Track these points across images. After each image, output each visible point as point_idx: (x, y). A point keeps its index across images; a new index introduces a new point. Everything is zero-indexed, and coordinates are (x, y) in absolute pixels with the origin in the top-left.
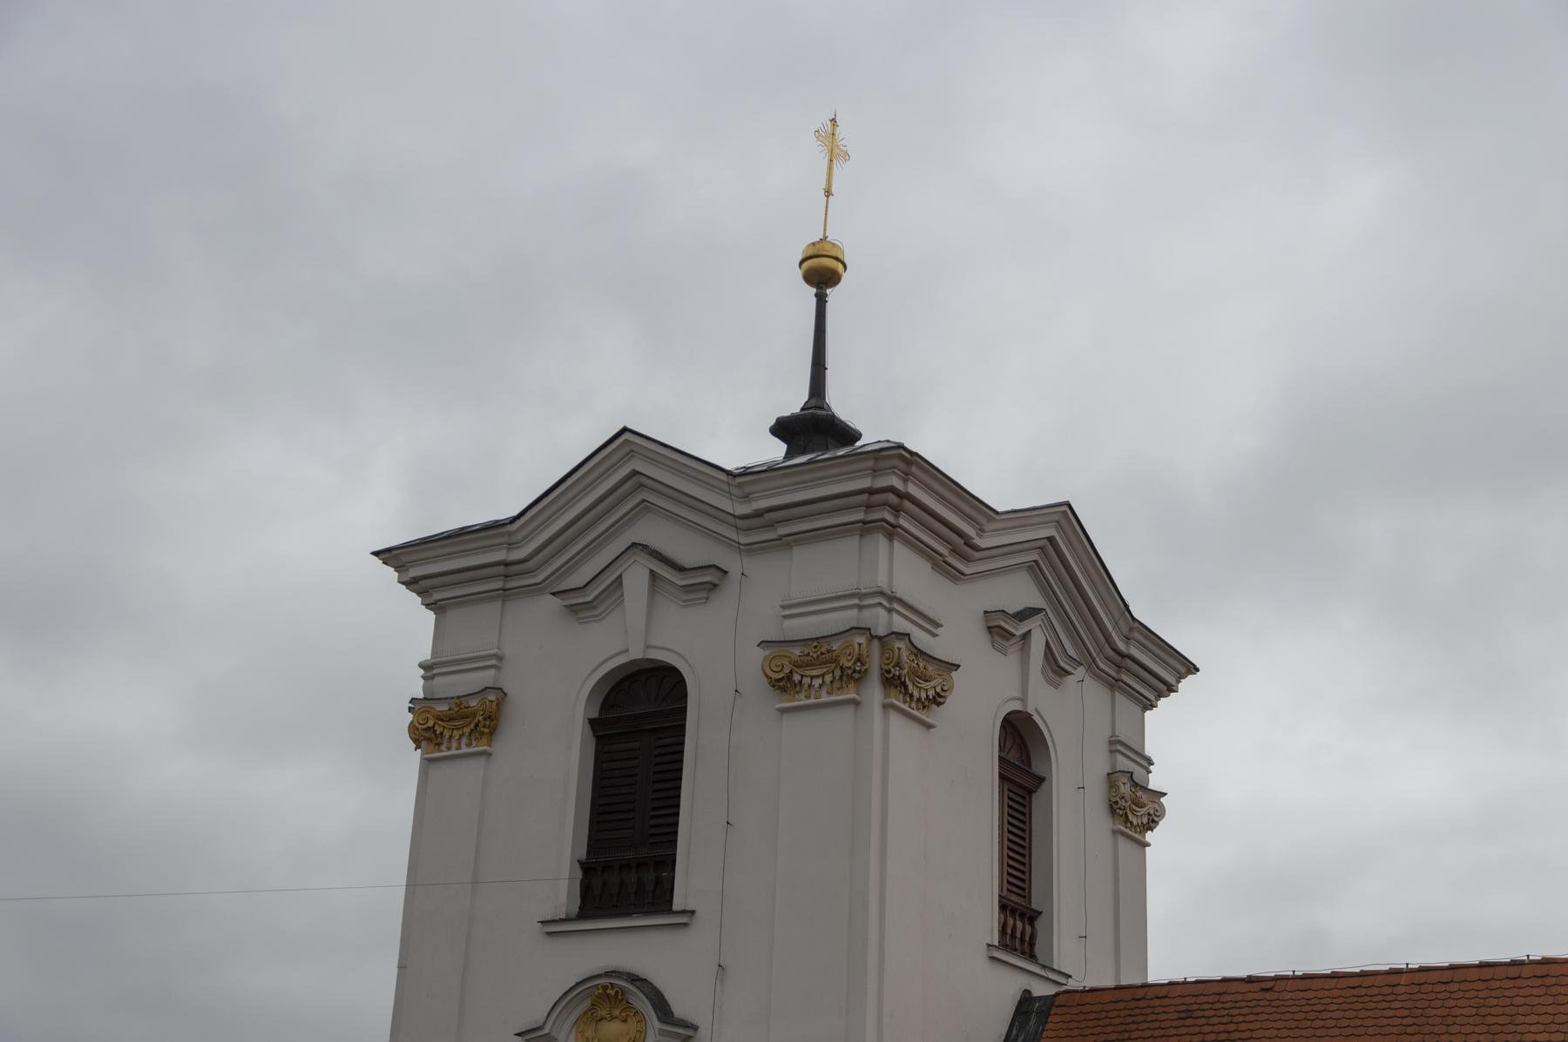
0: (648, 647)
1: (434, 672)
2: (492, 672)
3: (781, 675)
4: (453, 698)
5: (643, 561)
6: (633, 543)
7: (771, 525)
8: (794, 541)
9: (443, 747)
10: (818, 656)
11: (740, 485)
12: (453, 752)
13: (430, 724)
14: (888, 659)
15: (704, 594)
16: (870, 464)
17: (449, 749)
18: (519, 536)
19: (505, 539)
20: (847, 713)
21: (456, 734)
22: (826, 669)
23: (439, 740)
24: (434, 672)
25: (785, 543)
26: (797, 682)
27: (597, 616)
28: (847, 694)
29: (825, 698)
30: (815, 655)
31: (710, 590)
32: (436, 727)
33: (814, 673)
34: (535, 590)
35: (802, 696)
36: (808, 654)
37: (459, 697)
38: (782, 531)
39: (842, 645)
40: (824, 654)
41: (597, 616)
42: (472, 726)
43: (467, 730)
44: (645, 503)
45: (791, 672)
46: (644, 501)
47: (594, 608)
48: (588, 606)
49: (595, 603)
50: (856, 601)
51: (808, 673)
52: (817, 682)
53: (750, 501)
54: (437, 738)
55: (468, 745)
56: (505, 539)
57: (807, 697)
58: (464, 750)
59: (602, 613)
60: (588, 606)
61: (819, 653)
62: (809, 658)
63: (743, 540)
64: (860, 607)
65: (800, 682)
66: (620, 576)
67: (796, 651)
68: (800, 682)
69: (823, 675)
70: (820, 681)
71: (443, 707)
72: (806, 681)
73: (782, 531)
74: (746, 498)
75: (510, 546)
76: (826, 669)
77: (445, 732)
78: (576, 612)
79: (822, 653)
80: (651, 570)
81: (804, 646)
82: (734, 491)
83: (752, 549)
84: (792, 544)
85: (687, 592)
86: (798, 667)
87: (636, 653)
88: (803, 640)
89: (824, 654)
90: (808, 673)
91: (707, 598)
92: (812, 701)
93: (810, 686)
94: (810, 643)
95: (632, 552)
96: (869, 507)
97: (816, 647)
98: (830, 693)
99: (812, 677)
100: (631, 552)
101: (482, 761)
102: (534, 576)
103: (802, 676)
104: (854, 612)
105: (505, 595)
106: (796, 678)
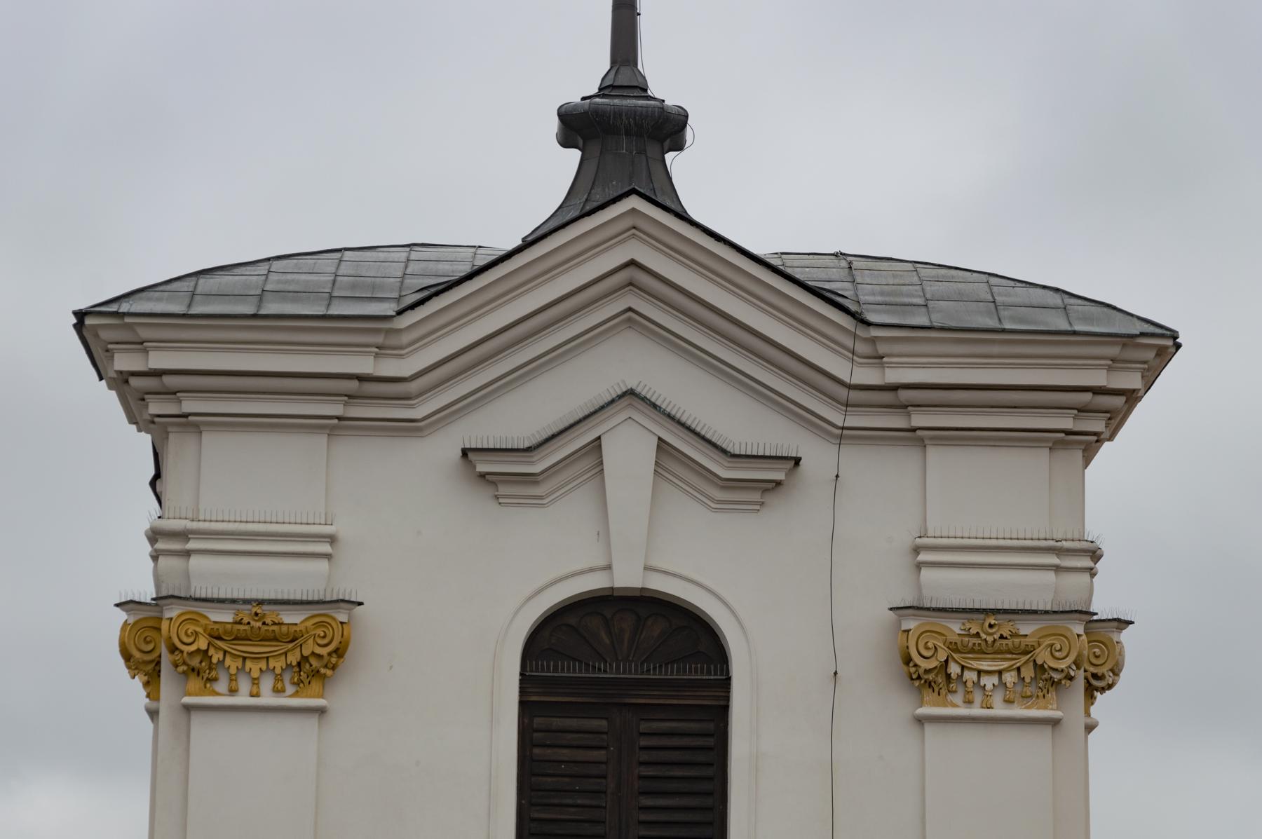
0: (648, 568)
1: (192, 545)
2: (323, 565)
3: (932, 664)
4: (247, 602)
5: (637, 416)
6: (631, 393)
7: (904, 407)
8: (932, 438)
9: (222, 686)
10: (995, 640)
11: (873, 341)
12: (242, 699)
13: (202, 644)
14: (1097, 657)
15: (756, 496)
16: (1114, 351)
17: (233, 691)
18: (405, 338)
19: (379, 339)
20: (1040, 740)
21: (254, 667)
22: (1006, 664)
23: (213, 674)
24: (192, 545)
25: (915, 438)
26: (954, 676)
27: (541, 497)
28: (1046, 708)
29: (1000, 710)
30: (990, 639)
31: (765, 491)
32: (211, 652)
33: (985, 665)
34: (411, 428)
35: (958, 698)
36: (978, 635)
37: (261, 602)
38: (919, 420)
39: (1041, 629)
40: (1006, 638)
41: (541, 497)
42: (293, 658)
43: (278, 664)
44: (630, 314)
45: (946, 661)
46: (630, 309)
47: (536, 483)
48: (529, 479)
49: (540, 478)
50: (1053, 560)
51: (976, 664)
52: (988, 681)
53: (882, 366)
54: (211, 669)
55: (278, 691)
56: (379, 339)
57: (969, 702)
58: (267, 699)
59: (548, 495)
60: (529, 479)
61: (996, 636)
62: (977, 641)
63: (836, 417)
64: (1058, 569)
65: (960, 676)
66: (599, 438)
67: (955, 627)
68: (960, 676)
69: (1000, 673)
70: (995, 680)
71: (224, 616)
72: (970, 676)
73: (919, 420)
74: (878, 359)
75: (382, 351)
76: (1006, 664)
77: (228, 661)
78: (494, 484)
79: (1002, 637)
80: (660, 439)
81: (970, 620)
82: (861, 348)
83: (844, 436)
84: (927, 442)
85: (723, 488)
86: (957, 651)
87: (628, 577)
88: (964, 611)
89: (1006, 638)
90: (976, 664)
91: (762, 504)
92: (976, 711)
93: (977, 684)
94: (982, 616)
95: (626, 403)
96: (1082, 410)
97: (991, 626)
98: (1009, 702)
99: (980, 672)
100: (625, 401)
101: (311, 722)
102: (412, 407)
103: (963, 668)
104: (1050, 576)
105: (338, 426)
106: (954, 669)
